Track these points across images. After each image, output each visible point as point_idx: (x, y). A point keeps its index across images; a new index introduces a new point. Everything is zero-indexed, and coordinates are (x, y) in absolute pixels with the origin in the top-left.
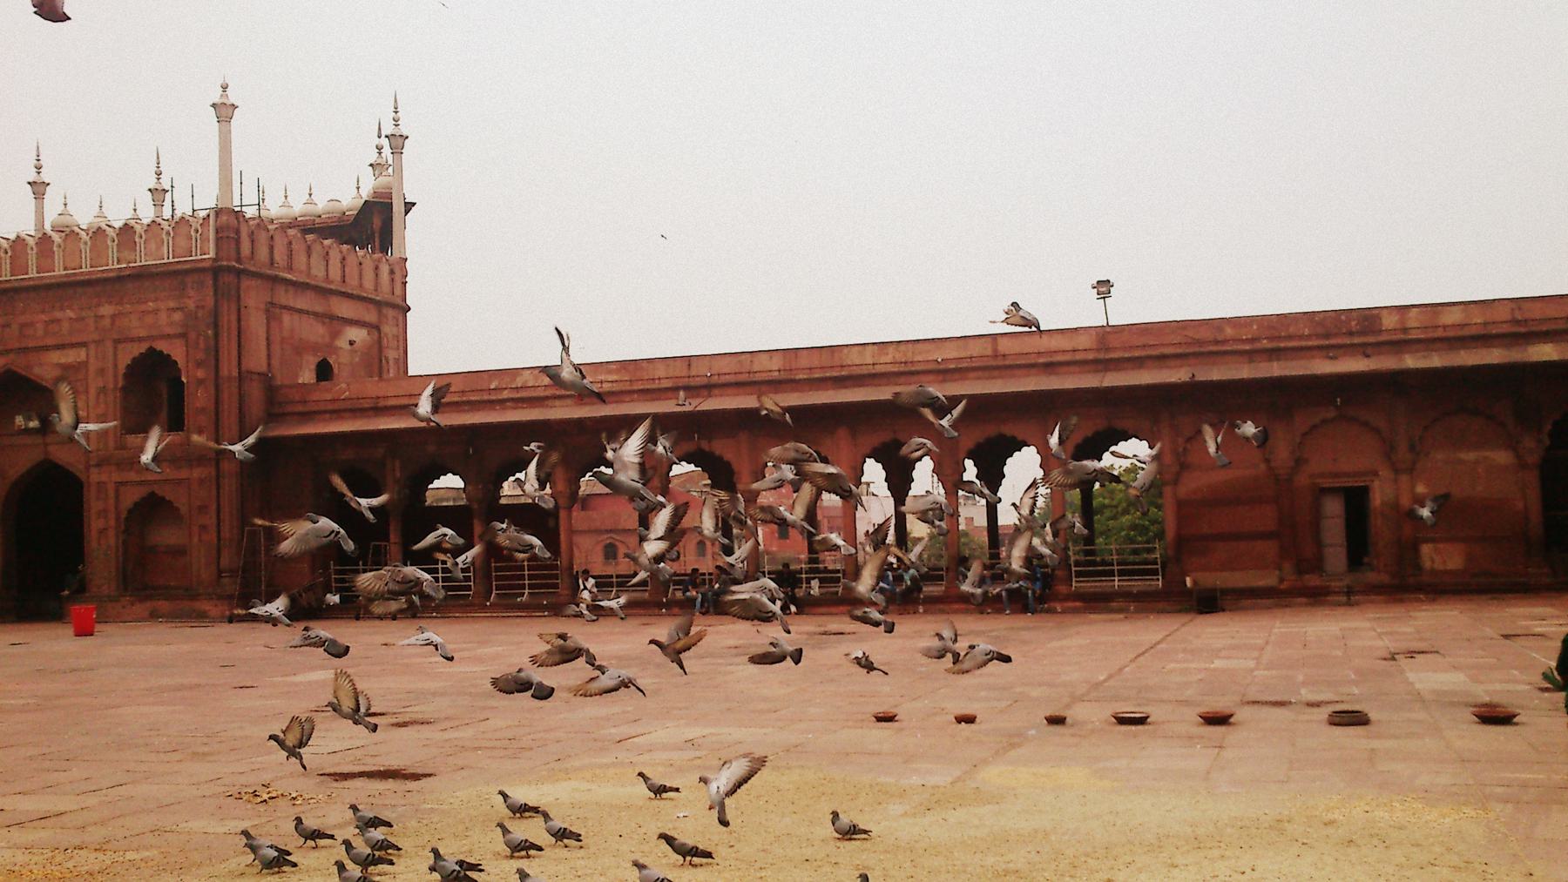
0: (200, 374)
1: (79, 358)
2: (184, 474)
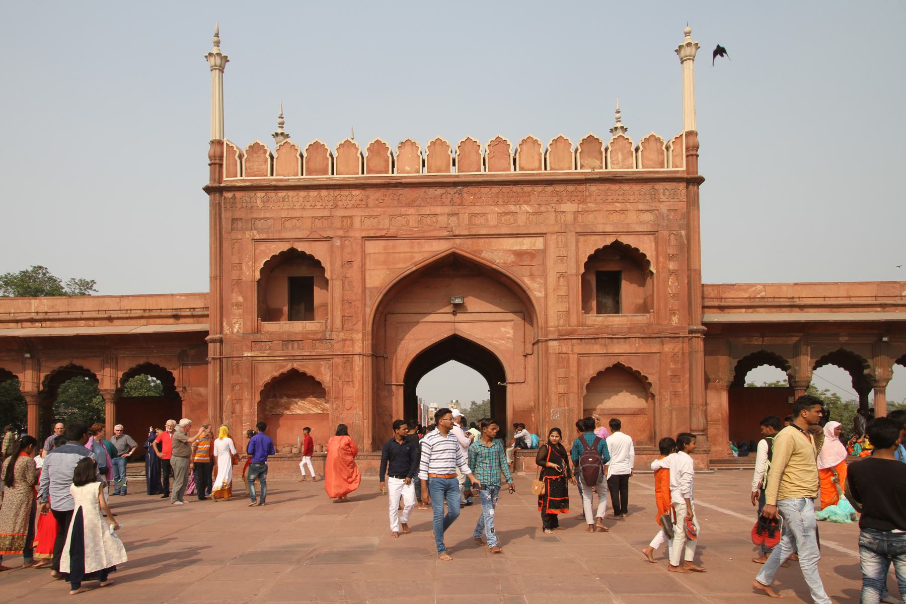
0: (672, 266)
1: (534, 246)
2: (655, 347)
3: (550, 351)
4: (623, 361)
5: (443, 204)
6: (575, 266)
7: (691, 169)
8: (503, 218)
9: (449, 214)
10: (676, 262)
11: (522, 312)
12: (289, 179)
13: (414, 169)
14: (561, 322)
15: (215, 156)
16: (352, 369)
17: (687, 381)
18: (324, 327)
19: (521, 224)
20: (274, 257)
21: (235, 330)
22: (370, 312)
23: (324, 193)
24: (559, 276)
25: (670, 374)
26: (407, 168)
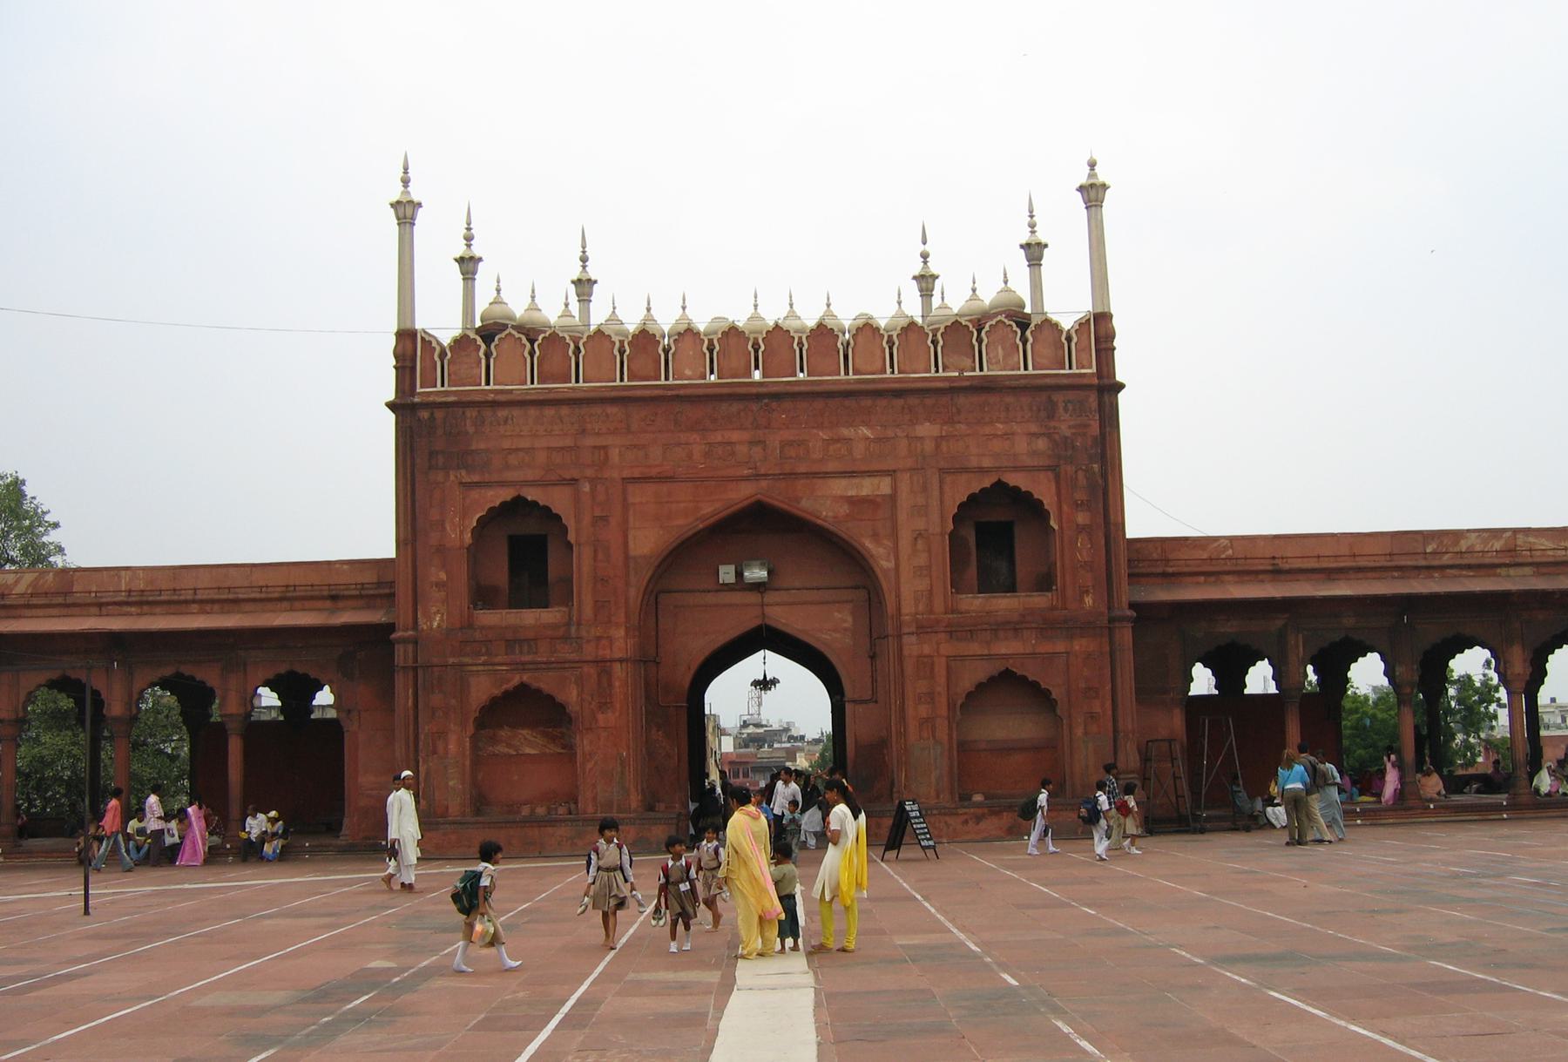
0: (1082, 518)
3: (906, 652)
4: (1010, 664)
5: (742, 428)
6: (938, 522)
7: (1105, 373)
8: (831, 448)
9: (750, 443)
10: (1088, 513)
11: (864, 588)
12: (512, 390)
13: (699, 373)
14: (921, 608)
15: (404, 355)
16: (610, 685)
17: (1109, 697)
18: (567, 617)
19: (859, 457)
20: (491, 509)
21: (435, 625)
22: (634, 594)
23: (565, 411)
24: (915, 536)
25: (1084, 686)
26: (688, 372)
